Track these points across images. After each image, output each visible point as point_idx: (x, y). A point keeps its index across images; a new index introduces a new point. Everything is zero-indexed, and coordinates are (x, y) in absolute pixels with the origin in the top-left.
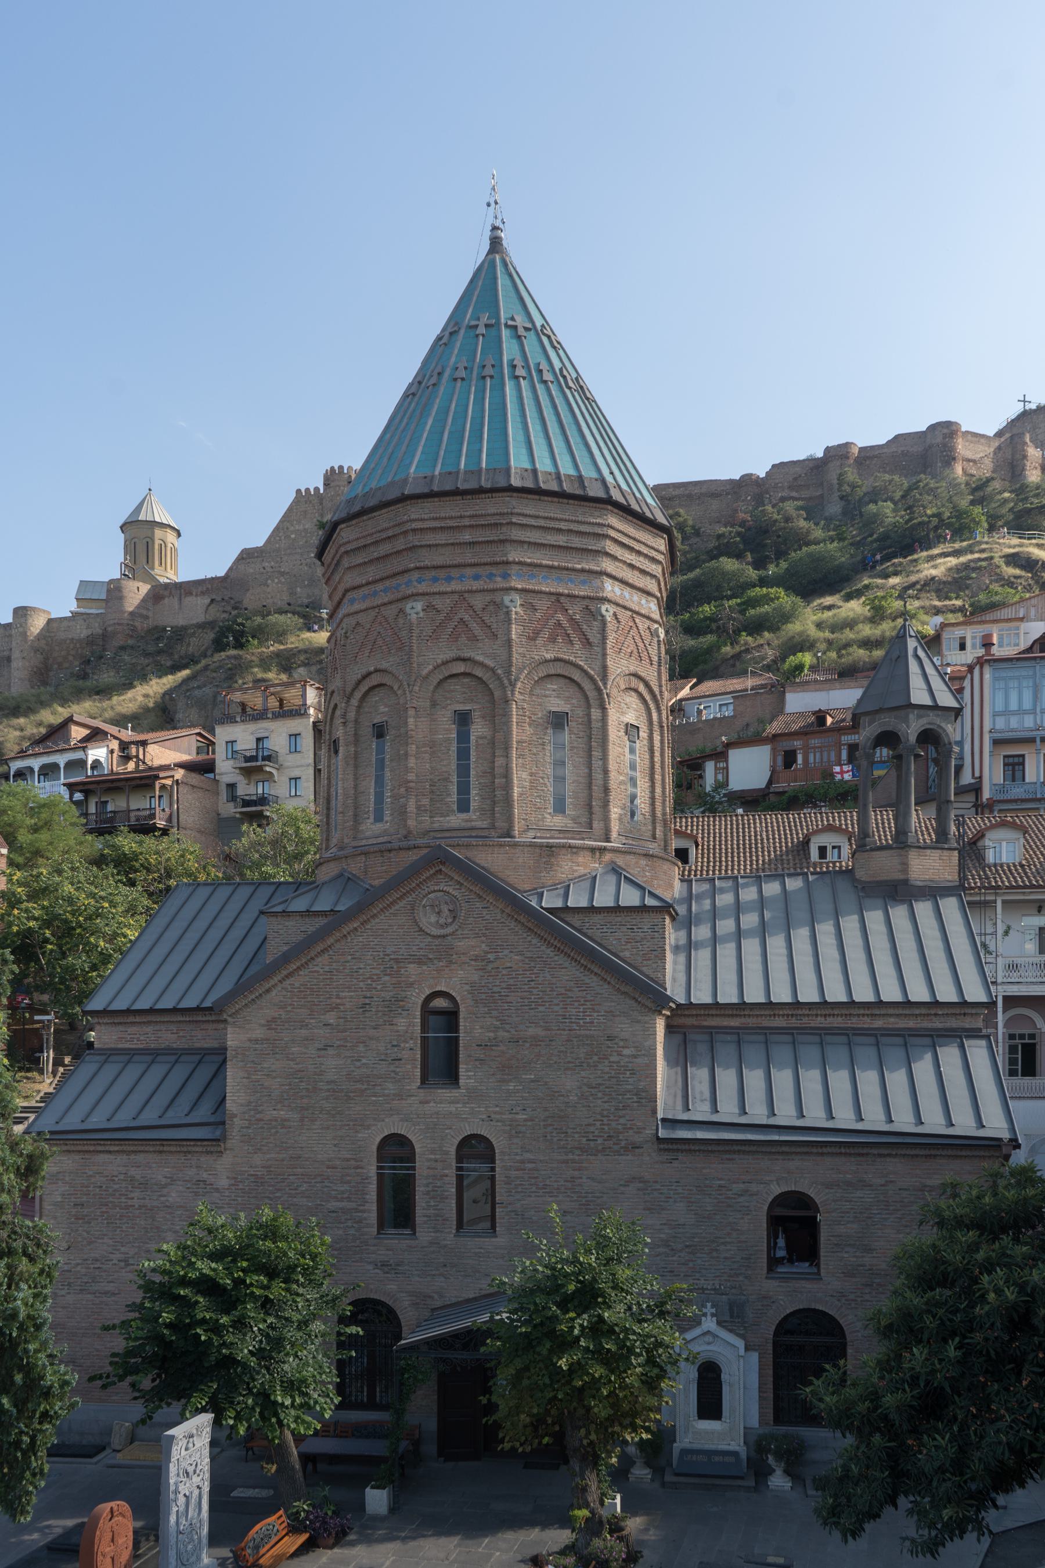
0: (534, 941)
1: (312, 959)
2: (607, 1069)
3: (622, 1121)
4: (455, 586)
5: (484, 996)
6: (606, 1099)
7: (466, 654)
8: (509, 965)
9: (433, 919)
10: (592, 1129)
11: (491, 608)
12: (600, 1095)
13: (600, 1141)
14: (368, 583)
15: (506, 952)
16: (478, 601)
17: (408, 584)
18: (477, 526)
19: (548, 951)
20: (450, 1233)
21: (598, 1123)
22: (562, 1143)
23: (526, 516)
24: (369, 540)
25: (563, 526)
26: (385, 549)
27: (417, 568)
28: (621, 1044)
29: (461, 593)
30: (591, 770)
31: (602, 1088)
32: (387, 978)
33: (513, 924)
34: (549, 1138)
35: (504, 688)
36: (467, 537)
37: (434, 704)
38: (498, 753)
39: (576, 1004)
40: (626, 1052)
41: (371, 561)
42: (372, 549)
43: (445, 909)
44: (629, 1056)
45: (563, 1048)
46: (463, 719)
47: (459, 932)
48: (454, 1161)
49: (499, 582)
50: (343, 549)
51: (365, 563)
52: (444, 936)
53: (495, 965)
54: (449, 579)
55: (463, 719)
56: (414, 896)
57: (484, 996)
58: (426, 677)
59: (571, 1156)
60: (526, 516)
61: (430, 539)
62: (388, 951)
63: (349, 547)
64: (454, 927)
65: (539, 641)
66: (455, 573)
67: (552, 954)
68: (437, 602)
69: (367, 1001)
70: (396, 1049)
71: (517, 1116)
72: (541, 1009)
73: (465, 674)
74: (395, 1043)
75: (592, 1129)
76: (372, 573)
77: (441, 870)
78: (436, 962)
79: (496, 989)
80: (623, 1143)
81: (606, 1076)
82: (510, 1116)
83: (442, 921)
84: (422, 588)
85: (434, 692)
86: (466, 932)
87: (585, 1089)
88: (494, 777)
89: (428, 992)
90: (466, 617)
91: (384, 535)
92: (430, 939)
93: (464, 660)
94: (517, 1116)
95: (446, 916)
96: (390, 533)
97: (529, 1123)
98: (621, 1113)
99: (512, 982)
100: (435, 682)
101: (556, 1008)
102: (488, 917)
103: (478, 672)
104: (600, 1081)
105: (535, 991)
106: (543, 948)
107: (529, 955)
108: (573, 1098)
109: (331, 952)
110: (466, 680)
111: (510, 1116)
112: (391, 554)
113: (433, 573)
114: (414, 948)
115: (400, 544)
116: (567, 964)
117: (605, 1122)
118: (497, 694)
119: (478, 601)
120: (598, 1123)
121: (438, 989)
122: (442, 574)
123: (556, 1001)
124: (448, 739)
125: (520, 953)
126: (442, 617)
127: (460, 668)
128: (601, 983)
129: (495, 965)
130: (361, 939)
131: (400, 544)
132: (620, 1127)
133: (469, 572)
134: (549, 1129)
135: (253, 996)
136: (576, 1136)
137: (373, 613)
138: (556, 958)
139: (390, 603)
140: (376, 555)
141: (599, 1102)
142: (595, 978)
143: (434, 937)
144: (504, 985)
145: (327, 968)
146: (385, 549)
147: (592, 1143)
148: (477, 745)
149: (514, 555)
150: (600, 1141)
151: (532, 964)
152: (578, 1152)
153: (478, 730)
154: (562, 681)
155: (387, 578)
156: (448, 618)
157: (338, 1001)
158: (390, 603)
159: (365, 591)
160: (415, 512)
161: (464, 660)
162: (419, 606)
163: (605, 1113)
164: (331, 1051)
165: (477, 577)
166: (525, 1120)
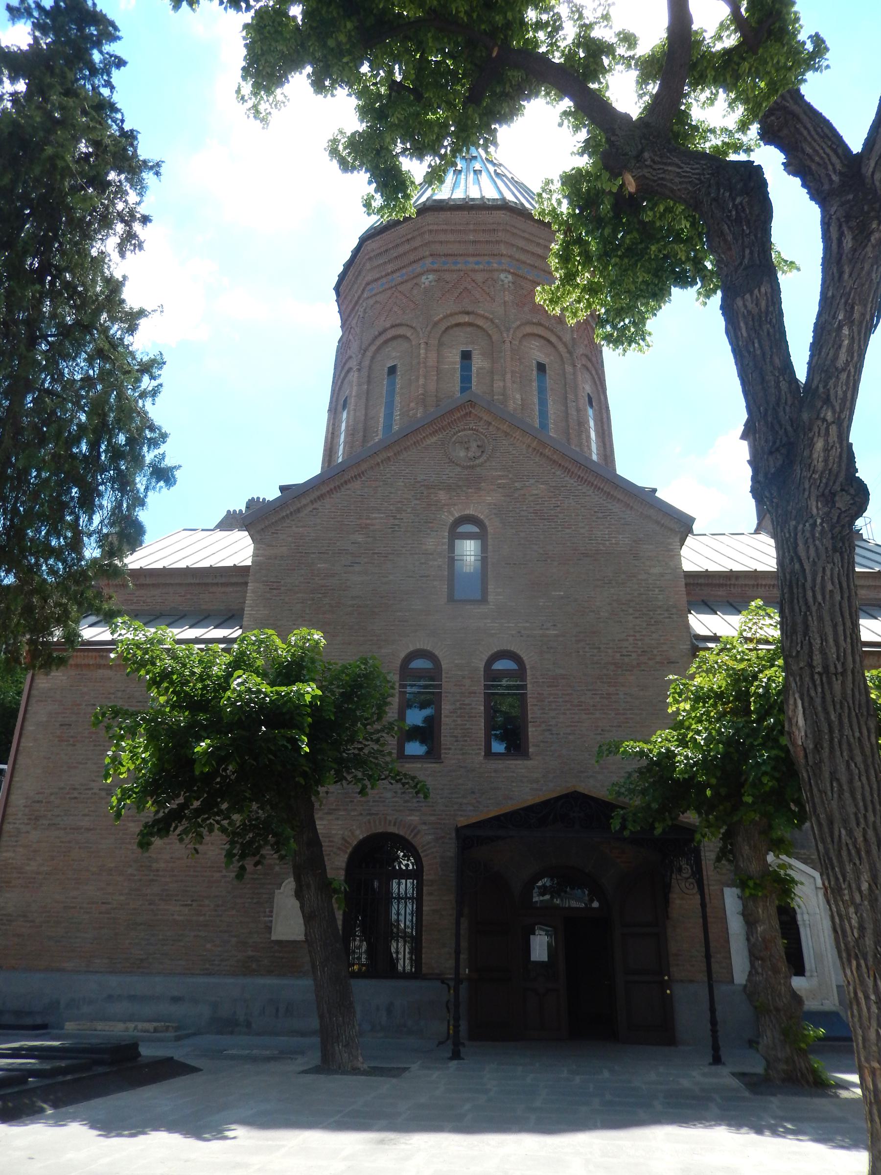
0: (558, 473)
1: (346, 482)
3: (654, 636)
4: (459, 266)
5: (511, 520)
7: (470, 309)
8: (535, 492)
9: (462, 454)
12: (631, 611)
13: (634, 656)
15: (532, 481)
16: (479, 278)
19: (572, 481)
20: (479, 754)
22: (595, 658)
26: (401, 250)
30: (567, 407)
32: (418, 502)
34: (581, 653)
37: (441, 344)
39: (602, 527)
42: (392, 251)
43: (474, 445)
46: (466, 356)
47: (488, 464)
48: (482, 679)
52: (472, 467)
54: (456, 263)
55: (466, 356)
56: (445, 433)
58: (436, 324)
61: (442, 237)
62: (419, 479)
64: (484, 457)
65: (526, 309)
66: (459, 259)
67: (575, 484)
68: (447, 276)
69: (397, 522)
70: (424, 566)
71: (548, 632)
72: (568, 531)
73: (470, 324)
74: (423, 561)
77: (470, 412)
78: (464, 489)
79: (523, 513)
80: (658, 659)
82: (541, 632)
83: (470, 454)
84: (435, 266)
85: (441, 336)
86: (494, 464)
89: (457, 515)
92: (459, 469)
94: (548, 632)
95: (474, 450)
97: (561, 639)
99: (538, 507)
100: (443, 328)
101: (582, 531)
102: (514, 452)
103: (480, 322)
105: (561, 516)
106: (566, 479)
109: (363, 478)
110: (469, 329)
111: (541, 632)
113: (443, 259)
114: (444, 477)
116: (590, 492)
117: (638, 638)
119: (479, 278)
120: (631, 639)
121: (467, 512)
124: (454, 368)
127: (466, 319)
128: (624, 509)
130: (393, 468)
132: (653, 642)
133: (471, 259)
135: (284, 514)
136: (610, 651)
137: (390, 292)
138: (580, 487)
139: (406, 281)
143: (464, 467)
144: (531, 510)
145: (359, 492)
146: (401, 250)
147: (626, 659)
151: (557, 492)
153: (478, 362)
154: (543, 342)
155: (404, 267)
157: (368, 521)
158: (406, 281)
159: (384, 280)
163: (637, 628)
164: (357, 568)
165: (477, 263)
166: (557, 636)
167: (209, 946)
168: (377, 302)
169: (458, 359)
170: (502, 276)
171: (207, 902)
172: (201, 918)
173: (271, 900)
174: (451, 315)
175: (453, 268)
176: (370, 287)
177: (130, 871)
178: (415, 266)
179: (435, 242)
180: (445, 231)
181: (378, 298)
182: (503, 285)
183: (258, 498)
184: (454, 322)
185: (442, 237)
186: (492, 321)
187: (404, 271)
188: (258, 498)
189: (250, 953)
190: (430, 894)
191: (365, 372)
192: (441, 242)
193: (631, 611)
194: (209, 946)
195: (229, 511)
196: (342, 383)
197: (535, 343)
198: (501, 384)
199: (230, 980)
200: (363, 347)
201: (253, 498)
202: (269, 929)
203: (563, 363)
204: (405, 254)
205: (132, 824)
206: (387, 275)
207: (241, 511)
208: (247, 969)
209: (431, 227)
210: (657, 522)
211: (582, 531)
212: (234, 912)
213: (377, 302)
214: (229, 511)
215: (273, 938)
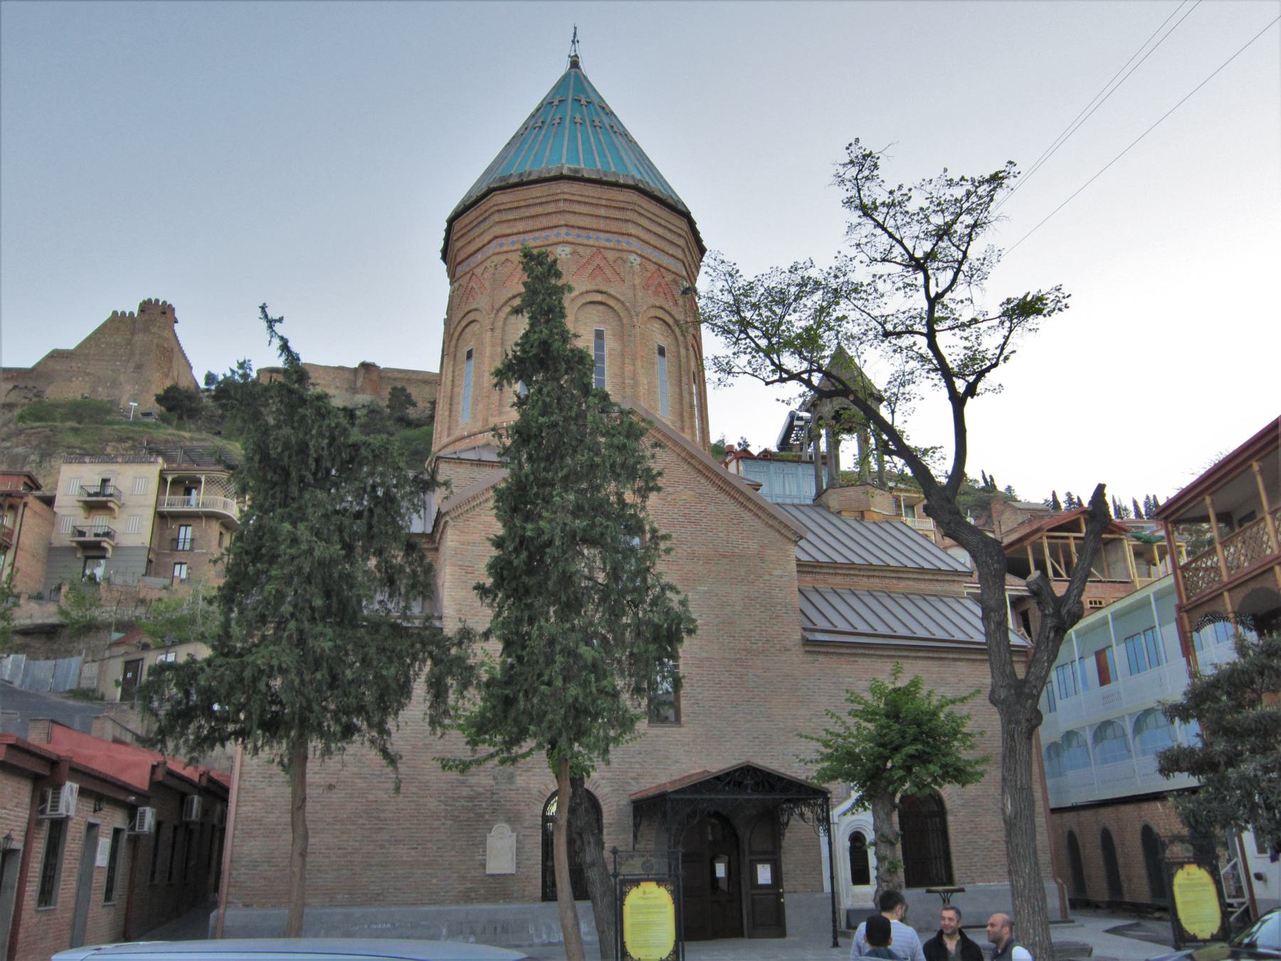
0: (703, 481)
2: (762, 585)
4: (591, 242)
5: (665, 521)
6: (763, 609)
7: (604, 289)
10: (753, 634)
11: (620, 262)
13: (760, 644)
14: (519, 233)
15: (681, 487)
17: (558, 235)
18: (610, 207)
19: (713, 490)
21: (758, 629)
23: (642, 208)
24: (522, 203)
25: (662, 222)
26: (534, 211)
27: (567, 226)
28: (771, 566)
29: (598, 248)
31: (759, 600)
33: (686, 467)
35: (631, 317)
36: (602, 212)
38: (627, 361)
40: (777, 572)
41: (521, 219)
42: (523, 210)
44: (777, 576)
45: (728, 567)
49: (625, 246)
50: (496, 208)
51: (515, 220)
53: (673, 497)
54: (588, 238)
55: (599, 335)
57: (665, 521)
59: (738, 656)
60: (642, 208)
61: (576, 208)
63: (502, 207)
66: (591, 233)
68: (580, 249)
72: (710, 534)
73: (601, 303)
75: (753, 634)
76: (521, 226)
79: (675, 516)
80: (778, 647)
81: (762, 591)
84: (570, 239)
87: (746, 600)
88: (624, 378)
90: (602, 265)
91: (538, 201)
93: (601, 292)
96: (544, 200)
98: (774, 621)
99: (686, 511)
101: (721, 535)
103: (612, 303)
104: (757, 595)
105: (704, 520)
107: (699, 491)
108: (738, 608)
110: (601, 308)
112: (541, 215)
113: (577, 231)
115: (551, 208)
116: (727, 501)
118: (625, 321)
119: (611, 255)
122: (583, 233)
123: (721, 529)
125: (692, 489)
126: (584, 261)
127: (599, 298)
129: (673, 497)
131: (551, 208)
133: (602, 235)
134: (721, 632)
140: (527, 214)
141: (758, 612)
142: (748, 514)
146: (534, 211)
147: (755, 647)
148: (610, 355)
149: (632, 229)
150: (760, 644)
152: (744, 653)
155: (537, 230)
156: (588, 262)
160: (565, 187)
161: (601, 292)
162: (568, 249)
165: (608, 240)
167: (434, 881)
168: (507, 260)
169: (592, 337)
170: (632, 257)
171: (430, 845)
172: (426, 859)
173: (483, 843)
174: (587, 292)
175: (586, 242)
176: (499, 241)
177: (361, 821)
178: (547, 233)
179: (569, 212)
180: (579, 202)
181: (509, 256)
182: (631, 267)
183: (157, 301)
184: (588, 300)
185: (576, 208)
186: (622, 303)
187: (537, 234)
188: (157, 301)
189: (469, 885)
190: (609, 834)
191: (498, 333)
192: (575, 213)
193: (758, 606)
194: (434, 881)
195: (115, 313)
196: (463, 330)
197: (657, 325)
198: (631, 368)
199: (454, 907)
200: (497, 306)
201: (150, 300)
202: (484, 866)
203: (678, 345)
204: (537, 216)
205: (359, 781)
206: (519, 233)
207: (132, 314)
208: (467, 897)
209: (566, 197)
210: (779, 531)
211: (721, 535)
212: (453, 853)
213: (507, 260)
214: (115, 313)
215: (488, 872)
